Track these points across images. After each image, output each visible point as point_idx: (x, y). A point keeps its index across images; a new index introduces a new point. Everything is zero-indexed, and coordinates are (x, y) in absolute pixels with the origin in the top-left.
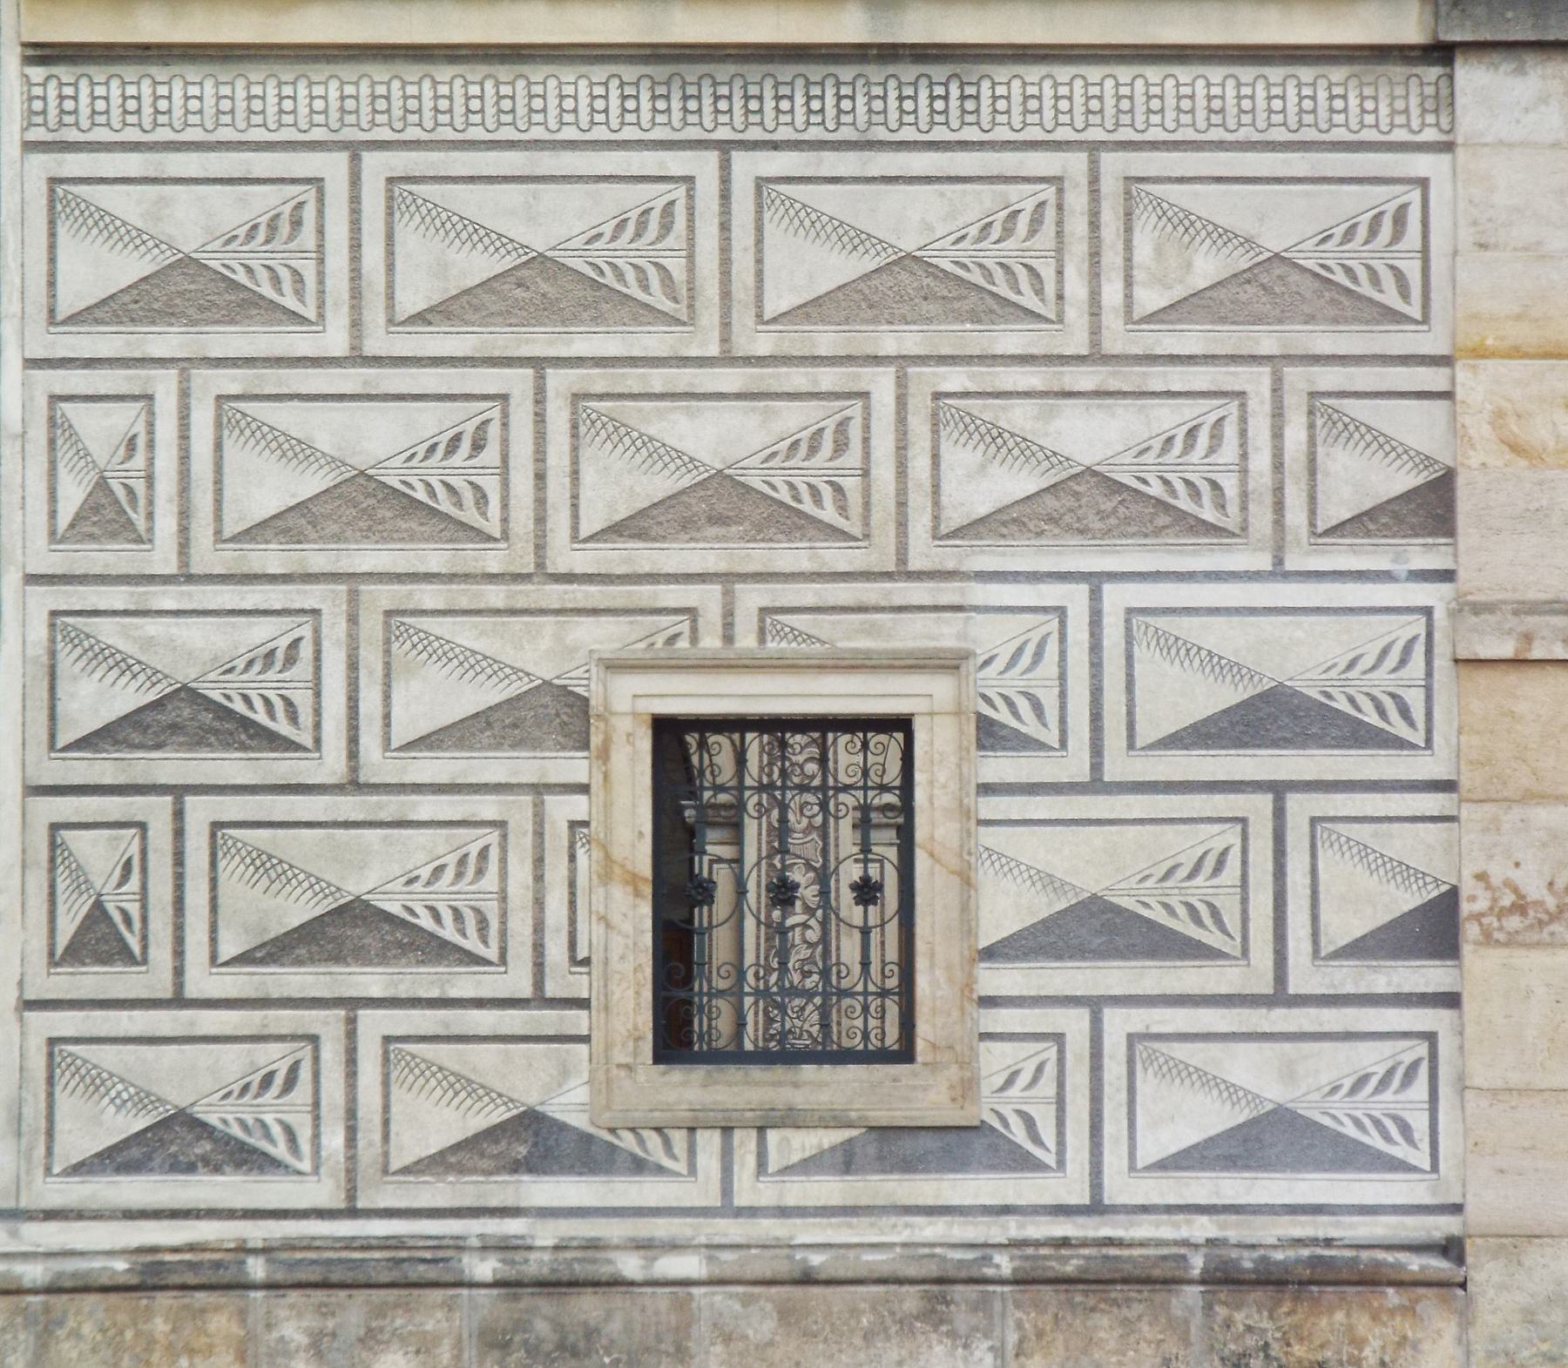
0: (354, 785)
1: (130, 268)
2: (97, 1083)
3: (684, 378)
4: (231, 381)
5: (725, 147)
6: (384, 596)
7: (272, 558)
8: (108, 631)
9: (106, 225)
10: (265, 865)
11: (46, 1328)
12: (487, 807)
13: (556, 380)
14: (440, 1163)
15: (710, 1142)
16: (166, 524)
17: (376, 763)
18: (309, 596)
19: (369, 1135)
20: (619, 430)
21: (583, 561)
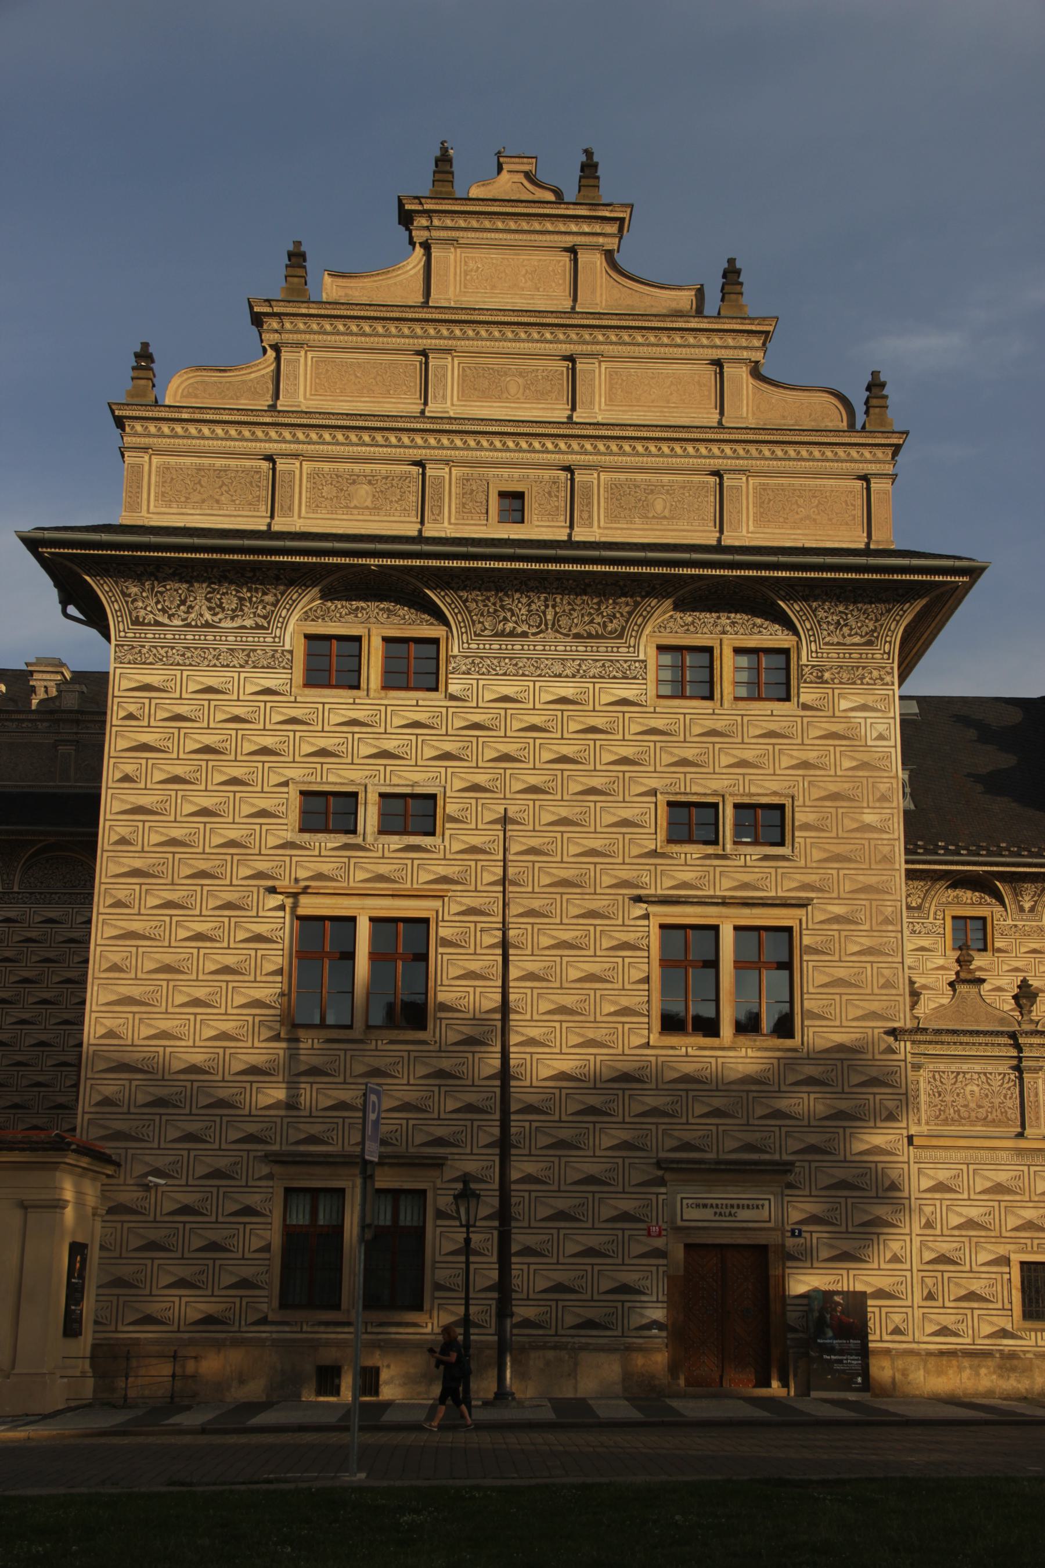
0: (971, 1271)
1: (931, 1183)
2: (931, 1321)
3: (1024, 1204)
4: (949, 1203)
5: (1029, 1166)
6: (974, 1240)
7: (956, 1232)
8: (930, 1244)
9: (928, 1176)
10: (957, 1284)
11: (925, 1362)
12: (993, 1276)
13: (1002, 1204)
14: (988, 1336)
15: (1033, 1334)
16: (939, 1226)
17: (975, 1268)
18: (963, 1239)
19: (976, 1331)
20: (1013, 1213)
21: (1008, 1234)
